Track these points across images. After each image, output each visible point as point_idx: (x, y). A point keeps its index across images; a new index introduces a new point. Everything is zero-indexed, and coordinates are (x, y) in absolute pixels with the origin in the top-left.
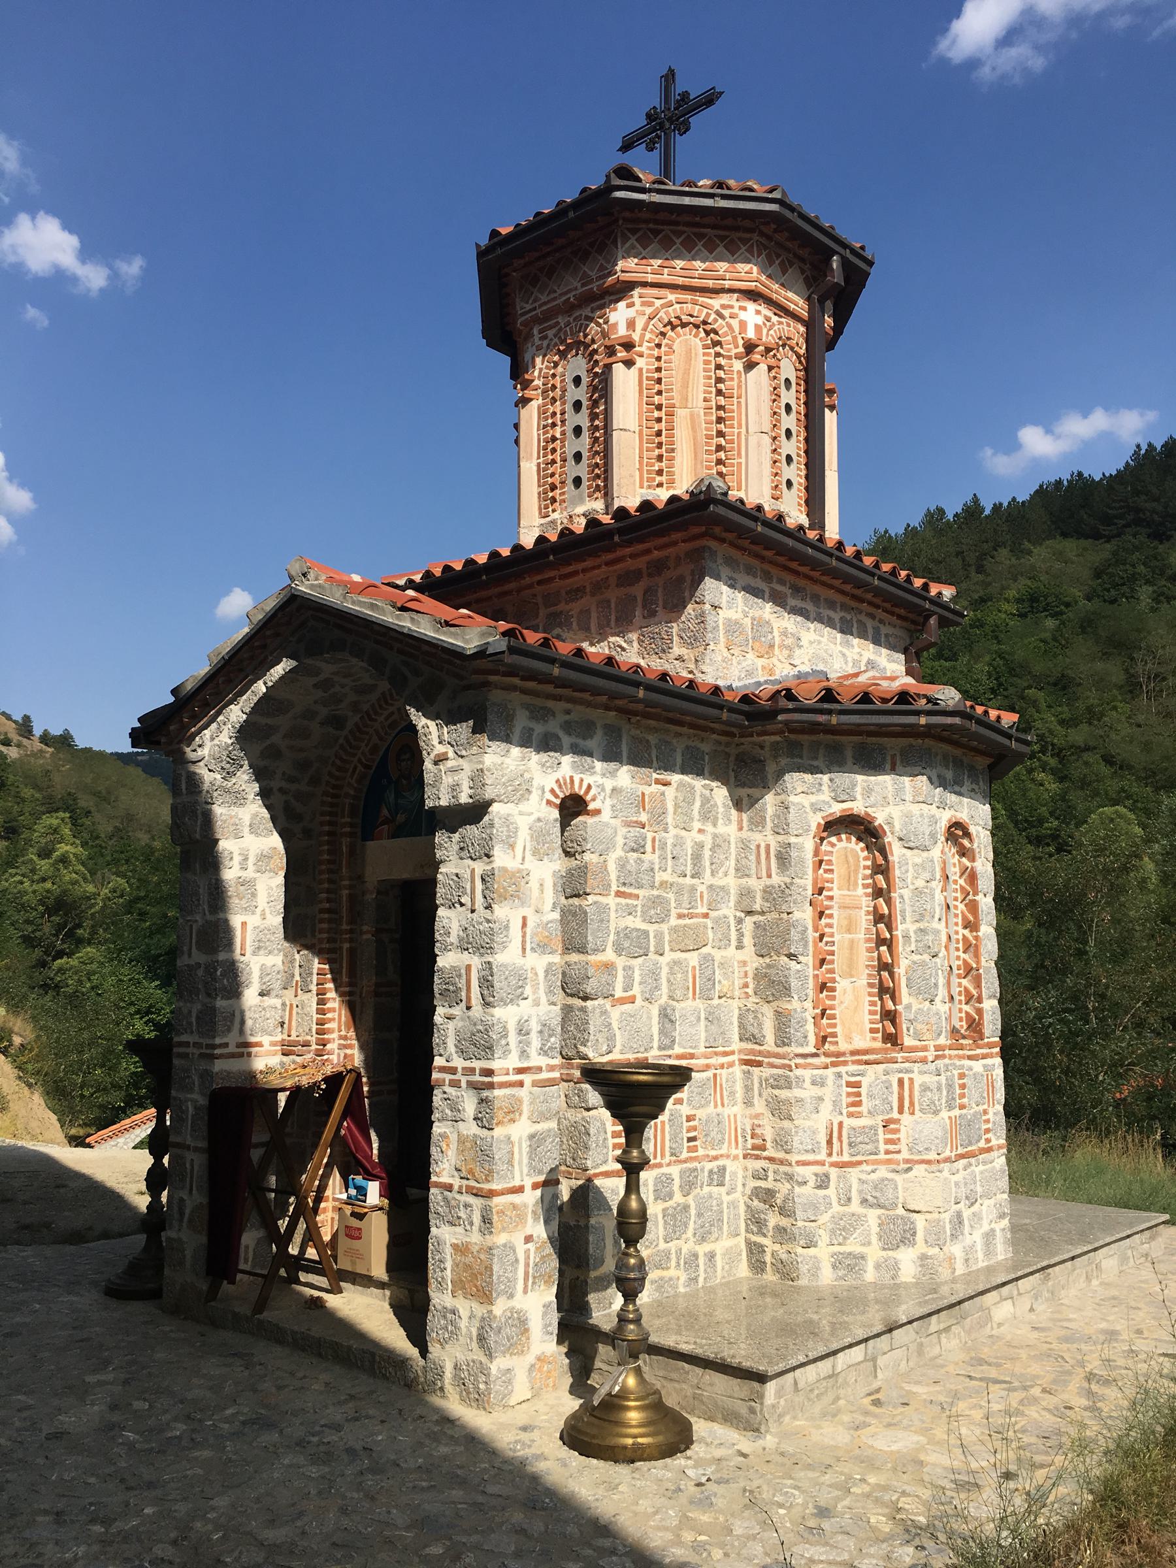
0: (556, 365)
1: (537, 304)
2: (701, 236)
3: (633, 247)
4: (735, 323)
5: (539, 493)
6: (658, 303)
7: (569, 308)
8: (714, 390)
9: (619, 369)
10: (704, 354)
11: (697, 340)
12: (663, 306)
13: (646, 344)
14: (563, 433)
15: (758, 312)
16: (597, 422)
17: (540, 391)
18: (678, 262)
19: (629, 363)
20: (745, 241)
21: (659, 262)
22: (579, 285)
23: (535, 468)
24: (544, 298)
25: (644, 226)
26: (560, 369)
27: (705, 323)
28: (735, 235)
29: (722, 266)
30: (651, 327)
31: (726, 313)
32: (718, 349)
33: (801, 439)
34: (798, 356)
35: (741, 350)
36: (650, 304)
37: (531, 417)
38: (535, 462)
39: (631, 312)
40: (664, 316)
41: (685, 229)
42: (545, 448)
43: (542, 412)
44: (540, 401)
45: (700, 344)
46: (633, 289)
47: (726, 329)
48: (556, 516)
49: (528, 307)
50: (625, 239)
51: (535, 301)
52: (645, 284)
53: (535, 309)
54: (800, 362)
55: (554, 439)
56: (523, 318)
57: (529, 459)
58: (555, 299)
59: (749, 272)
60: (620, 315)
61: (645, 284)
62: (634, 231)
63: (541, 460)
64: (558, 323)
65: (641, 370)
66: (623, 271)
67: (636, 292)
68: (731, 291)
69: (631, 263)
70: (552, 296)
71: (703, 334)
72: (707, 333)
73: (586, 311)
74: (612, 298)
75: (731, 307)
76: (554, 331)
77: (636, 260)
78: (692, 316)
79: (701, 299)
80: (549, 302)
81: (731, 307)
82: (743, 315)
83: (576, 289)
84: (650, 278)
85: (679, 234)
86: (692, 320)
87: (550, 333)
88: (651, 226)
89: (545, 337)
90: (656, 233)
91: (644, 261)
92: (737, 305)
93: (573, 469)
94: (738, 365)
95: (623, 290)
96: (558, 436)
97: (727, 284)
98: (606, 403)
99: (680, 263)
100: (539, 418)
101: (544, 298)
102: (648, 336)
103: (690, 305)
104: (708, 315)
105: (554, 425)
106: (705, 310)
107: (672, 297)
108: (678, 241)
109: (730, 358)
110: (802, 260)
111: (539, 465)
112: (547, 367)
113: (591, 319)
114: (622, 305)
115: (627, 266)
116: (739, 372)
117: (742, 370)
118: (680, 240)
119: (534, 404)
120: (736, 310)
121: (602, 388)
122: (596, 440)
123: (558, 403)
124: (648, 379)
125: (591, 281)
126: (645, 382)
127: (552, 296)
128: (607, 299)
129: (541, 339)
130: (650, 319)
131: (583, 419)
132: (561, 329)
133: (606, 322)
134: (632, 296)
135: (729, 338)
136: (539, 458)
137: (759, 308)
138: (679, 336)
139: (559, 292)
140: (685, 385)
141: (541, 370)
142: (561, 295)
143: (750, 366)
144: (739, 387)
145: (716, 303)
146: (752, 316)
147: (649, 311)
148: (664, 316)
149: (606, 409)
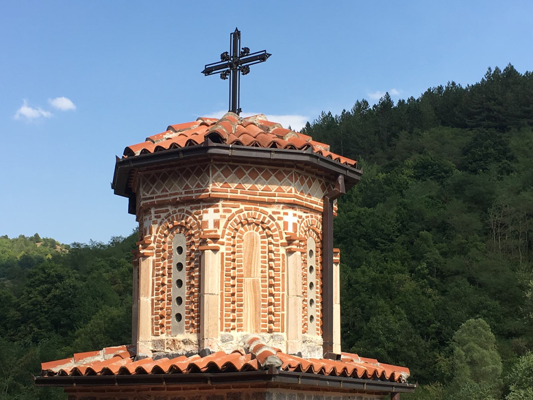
0: (166, 236)
1: (154, 195)
2: (261, 170)
3: (219, 176)
4: (281, 223)
5: (152, 319)
6: (234, 210)
7: (175, 203)
8: (267, 265)
9: (209, 254)
10: (262, 242)
11: (258, 233)
12: (237, 212)
13: (226, 236)
14: (169, 281)
15: (295, 215)
16: (193, 282)
17: (154, 251)
18: (247, 185)
19: (215, 250)
20: (287, 173)
21: (236, 185)
22: (183, 192)
23: (150, 302)
24: (159, 193)
25: (226, 163)
26: (168, 239)
27: (262, 223)
28: (281, 169)
29: (274, 188)
30: (229, 225)
31: (275, 217)
32: (270, 239)
33: (318, 286)
34: (317, 234)
35: (284, 241)
36: (230, 211)
37: (148, 267)
38: (150, 298)
39: (217, 216)
40: (238, 219)
41: (252, 165)
42: (157, 290)
43: (155, 265)
44: (154, 257)
45: (259, 236)
46: (218, 202)
47: (275, 227)
48: (163, 337)
49: (148, 196)
50: (215, 171)
51: (153, 193)
52: (226, 199)
53: (153, 198)
54: (318, 237)
55: (163, 284)
56: (145, 202)
57: (146, 295)
58: (166, 196)
59: (290, 190)
60: (209, 216)
61: (226, 199)
62: (220, 166)
63: (154, 297)
64: (168, 210)
65: (222, 254)
66: (212, 191)
67: (220, 203)
68: (279, 203)
69: (219, 186)
70: (165, 193)
71: (261, 230)
72: (264, 229)
73: (187, 208)
74: (204, 204)
75: (279, 213)
76: (166, 214)
77: (221, 184)
78: (254, 218)
79: (260, 208)
81: (279, 213)
82: (286, 218)
83: (181, 194)
84: (229, 195)
85: (247, 168)
86: (254, 220)
87: (163, 215)
88: (231, 163)
89: (159, 217)
90: (233, 167)
91: (225, 185)
92: (282, 211)
93: (176, 309)
94: (282, 251)
95: (211, 201)
96: (166, 282)
97: (276, 199)
98: (200, 271)
99: (247, 186)
100: (153, 268)
101: (159, 193)
102: (227, 231)
103: (253, 212)
104: (264, 218)
105: (163, 275)
106: (263, 215)
107: (242, 207)
108: (247, 173)
109: (277, 245)
110: (321, 176)
111: (152, 300)
112: (160, 236)
113: (190, 214)
114: (211, 210)
115: (215, 187)
116: (283, 255)
117: (285, 254)
118: (249, 171)
119: (151, 259)
120: (281, 215)
121: (197, 262)
122: (192, 293)
123: (166, 261)
124: (227, 259)
125: (191, 192)
126: (225, 261)
127: (165, 193)
128: (201, 205)
129: (156, 217)
130: (229, 220)
131: (183, 276)
132: (169, 215)
133: (201, 218)
134: (217, 206)
135: (277, 233)
136: (153, 295)
137: (295, 212)
138: (246, 230)
139: (170, 192)
140: (250, 263)
141: (155, 237)
142: (171, 195)
143: (290, 252)
144: (283, 265)
145: (269, 210)
146: (291, 217)
147: (228, 215)
148: (238, 219)
149: (200, 276)
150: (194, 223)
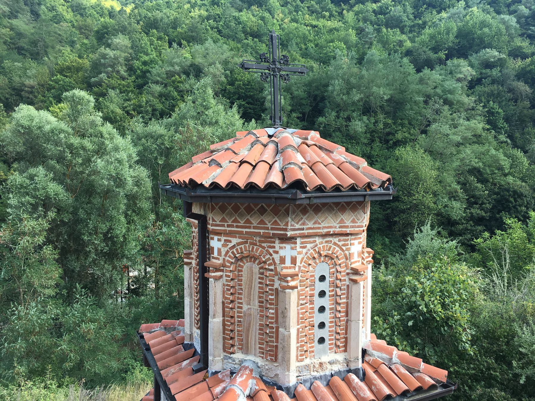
1: (305, 227)
5: (297, 348)
16: (339, 308)
22: (338, 226)
24: (310, 225)
48: (307, 361)
49: (297, 226)
51: (303, 224)
53: (303, 229)
56: (293, 233)
58: (319, 228)
64: (316, 241)
70: (317, 226)
76: (312, 245)
80: (313, 228)
83: (336, 227)
87: (309, 246)
89: (304, 247)
93: (319, 333)
101: (310, 225)
112: (304, 266)
125: (347, 227)
127: (317, 226)
128: (349, 237)
129: (301, 247)
132: (316, 246)
133: (348, 249)
139: (323, 225)
141: (300, 267)
142: (324, 227)
150: (341, 254)
